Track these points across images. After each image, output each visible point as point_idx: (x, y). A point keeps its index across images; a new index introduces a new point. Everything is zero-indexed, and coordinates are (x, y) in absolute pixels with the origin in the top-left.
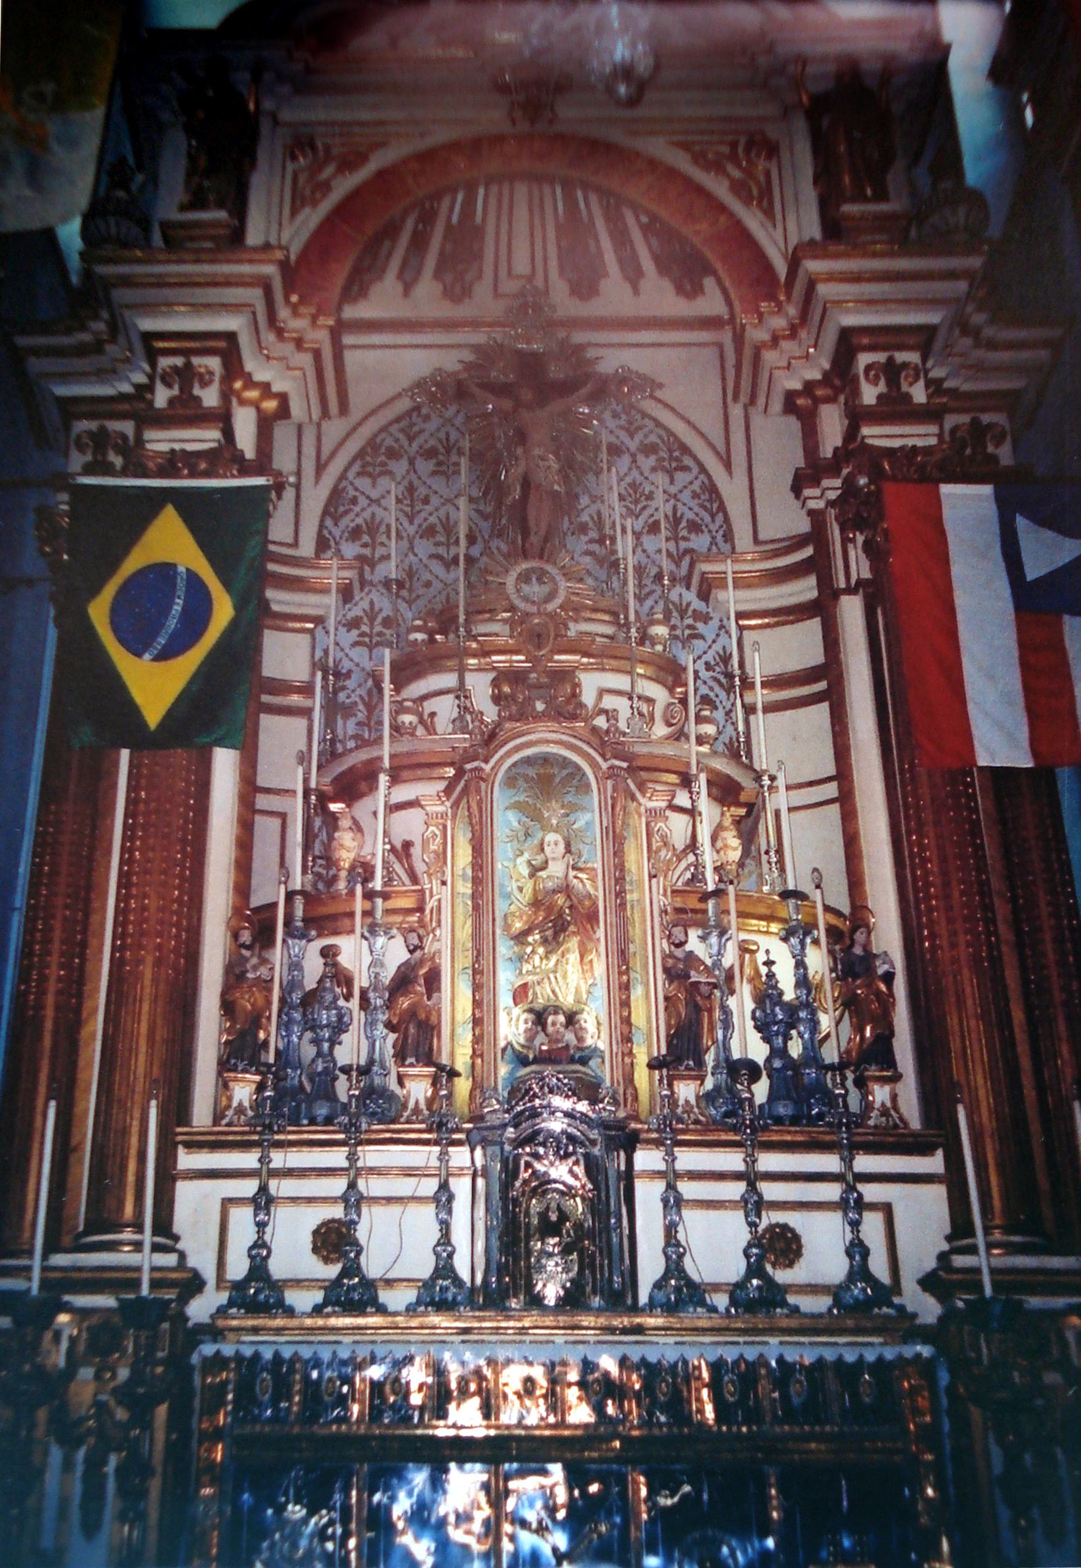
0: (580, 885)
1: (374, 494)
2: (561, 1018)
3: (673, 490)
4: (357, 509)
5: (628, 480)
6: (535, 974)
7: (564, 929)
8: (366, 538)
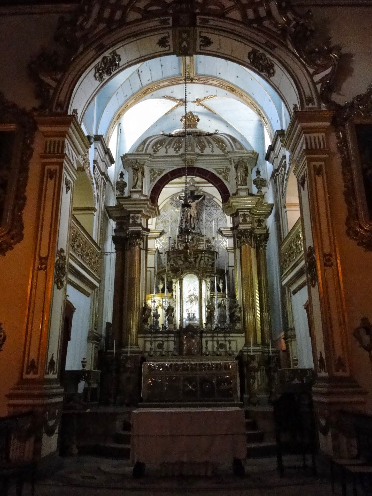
1: (165, 215)
2: (192, 315)
3: (217, 213)
4: (162, 218)
5: (209, 211)
7: (193, 301)
8: (164, 223)
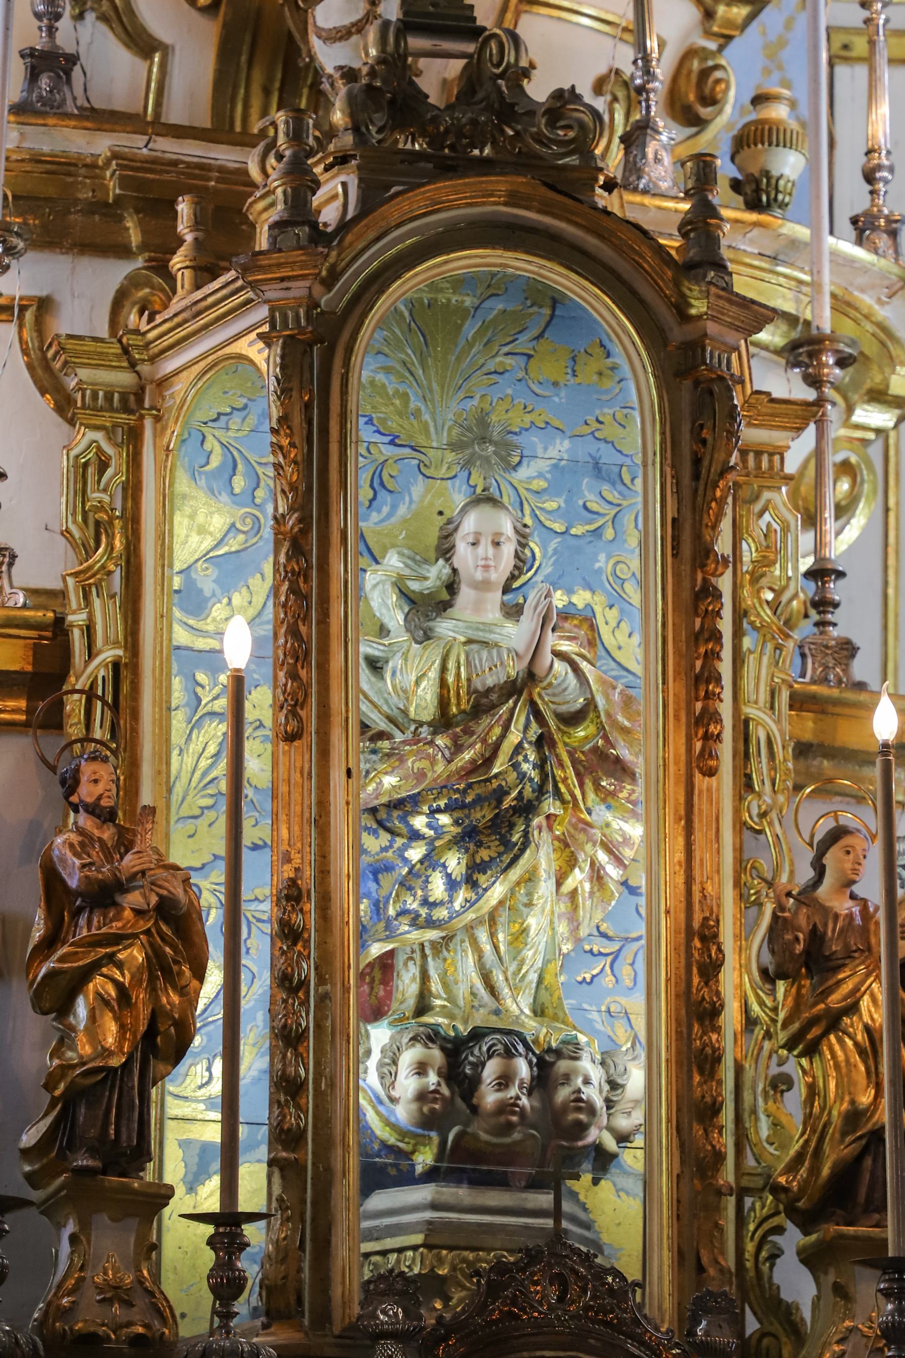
0: (572, 680)
2: (523, 1069)
6: (430, 923)
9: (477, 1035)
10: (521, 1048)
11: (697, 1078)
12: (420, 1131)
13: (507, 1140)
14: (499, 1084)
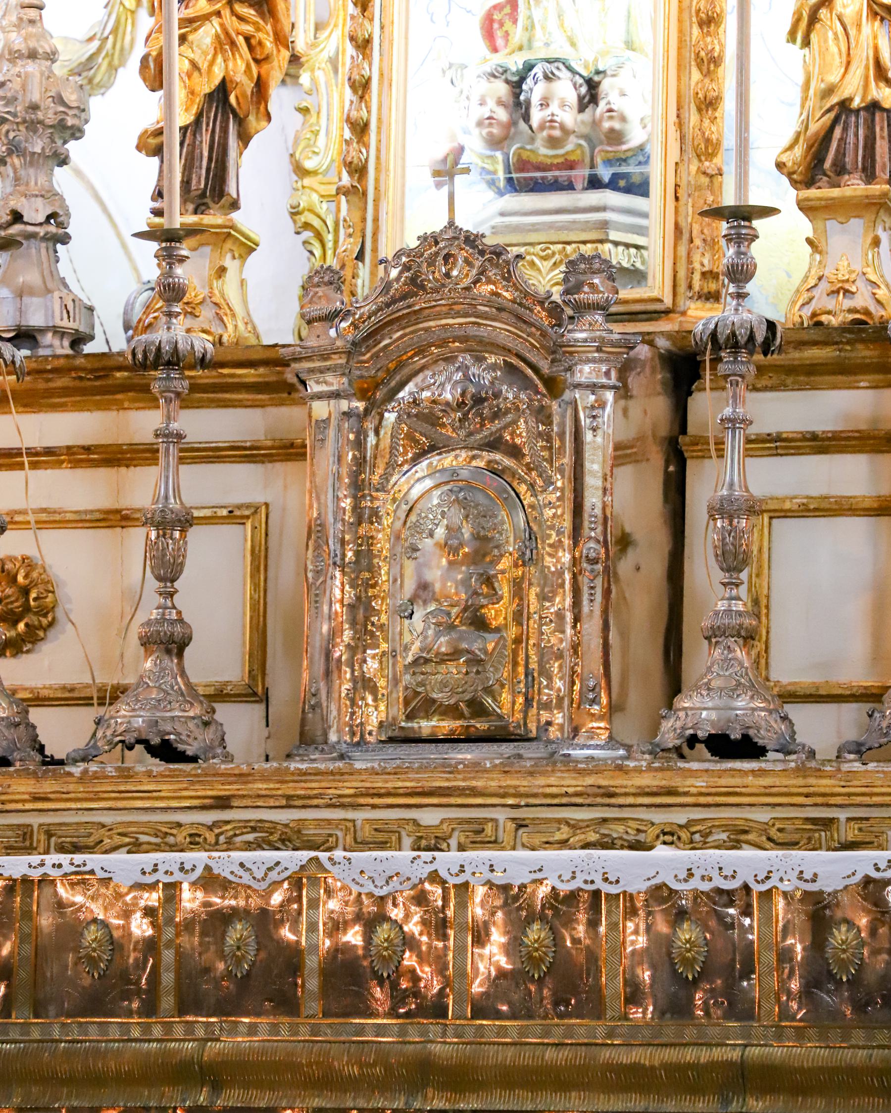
9: (529, 67)
10: (564, 74)
11: (696, 75)
12: (489, 153)
13: (561, 152)
14: (541, 105)
